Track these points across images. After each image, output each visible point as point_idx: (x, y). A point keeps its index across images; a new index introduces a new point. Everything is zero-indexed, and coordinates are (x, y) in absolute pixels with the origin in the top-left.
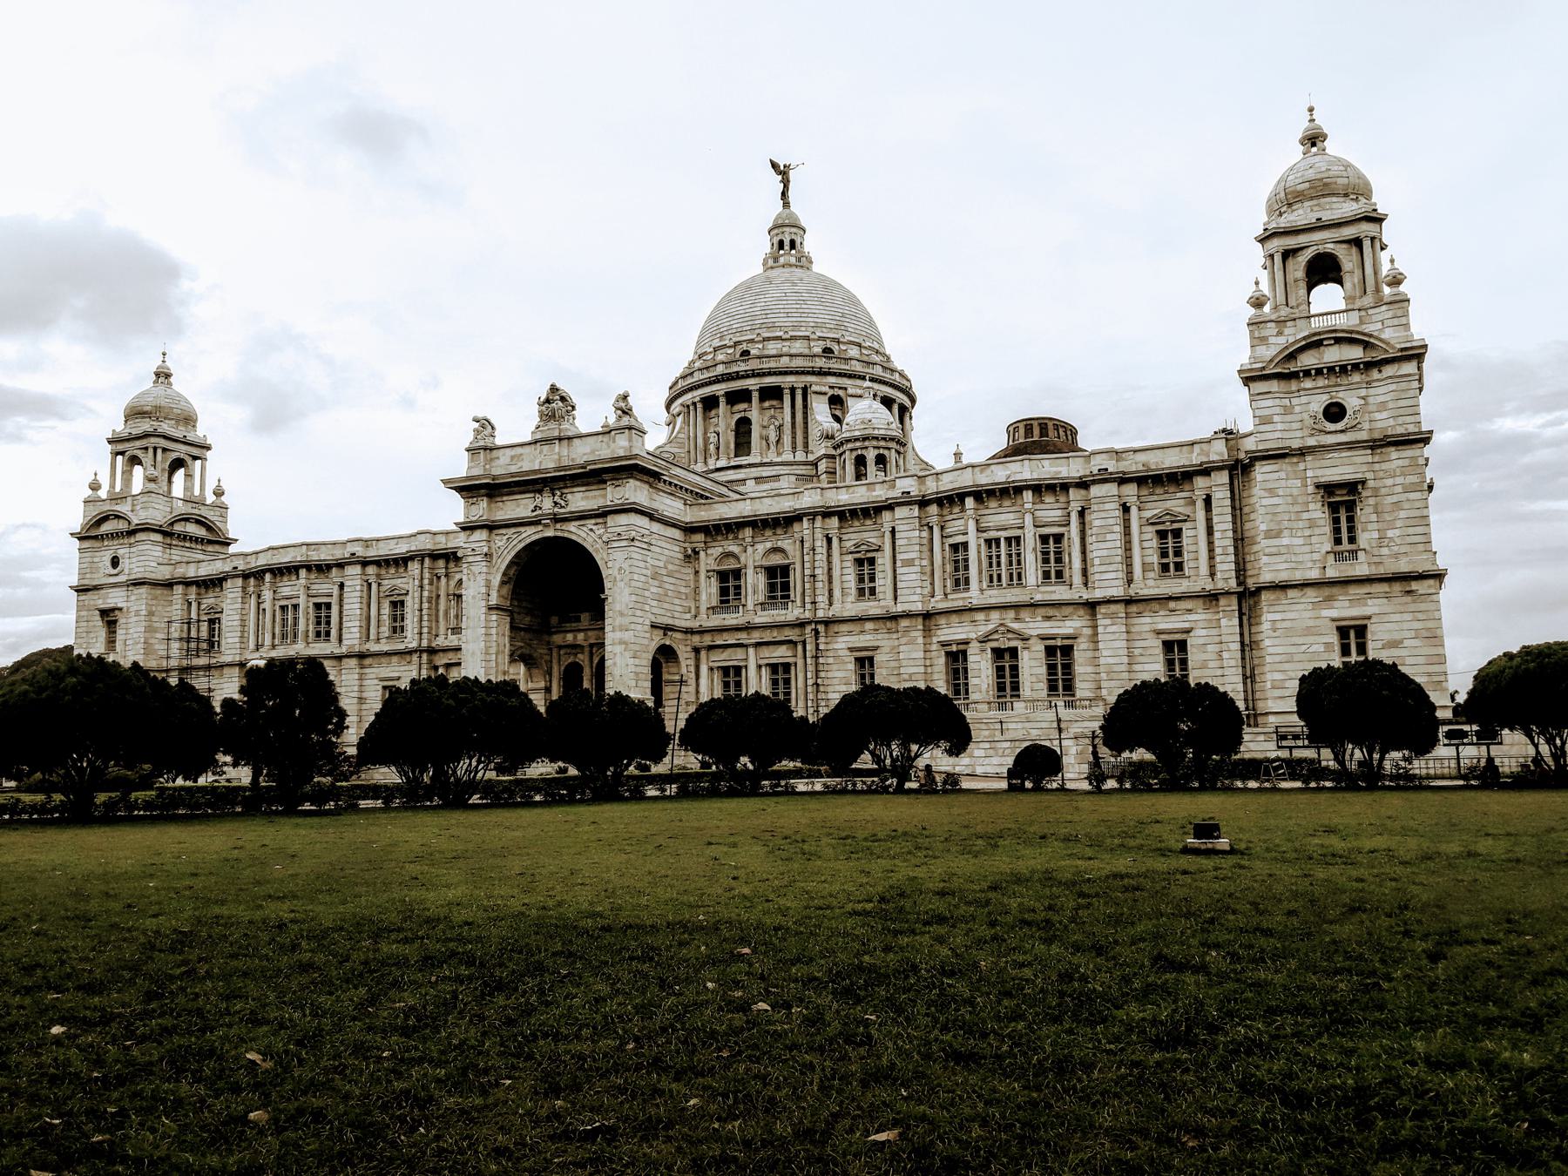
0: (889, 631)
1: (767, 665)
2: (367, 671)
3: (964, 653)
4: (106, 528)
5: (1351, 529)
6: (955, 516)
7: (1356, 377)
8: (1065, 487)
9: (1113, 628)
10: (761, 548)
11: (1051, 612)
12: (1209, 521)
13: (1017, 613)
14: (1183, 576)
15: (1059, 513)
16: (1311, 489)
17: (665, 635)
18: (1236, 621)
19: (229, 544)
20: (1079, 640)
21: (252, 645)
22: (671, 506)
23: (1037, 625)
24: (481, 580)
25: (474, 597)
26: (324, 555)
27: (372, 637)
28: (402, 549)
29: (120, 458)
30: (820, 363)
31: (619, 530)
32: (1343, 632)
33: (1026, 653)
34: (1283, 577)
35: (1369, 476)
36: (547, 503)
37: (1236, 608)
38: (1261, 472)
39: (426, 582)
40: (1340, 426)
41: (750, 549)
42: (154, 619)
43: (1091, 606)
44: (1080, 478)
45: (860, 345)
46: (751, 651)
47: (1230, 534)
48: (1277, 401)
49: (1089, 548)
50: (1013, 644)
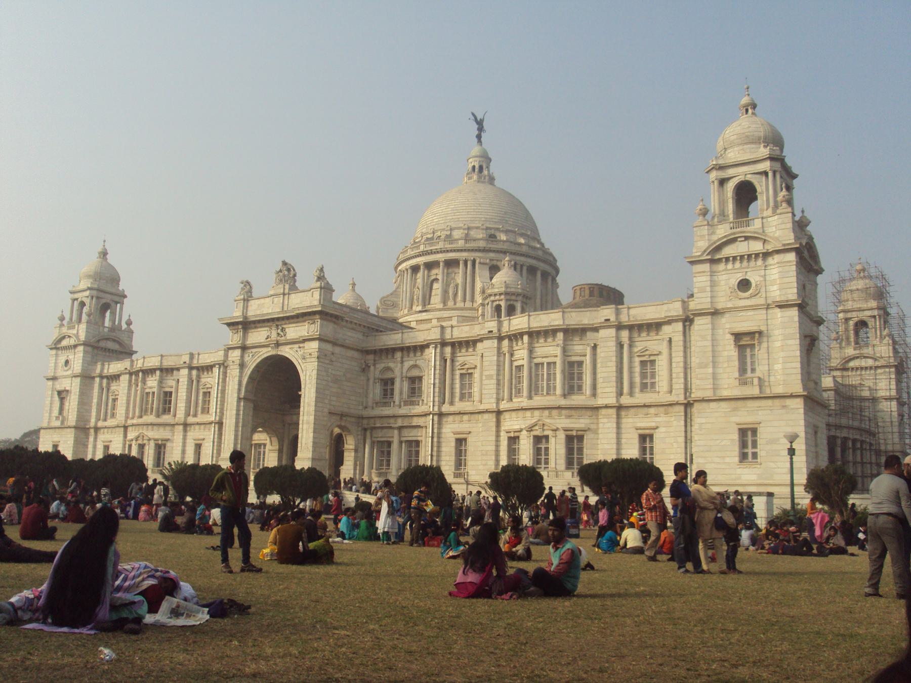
1: (407, 441)
2: (189, 434)
3: (518, 437)
4: (65, 343)
5: (752, 363)
7: (760, 262)
8: (582, 331)
9: (609, 425)
12: (670, 355)
13: (550, 413)
16: (729, 336)
17: (341, 419)
18: (683, 423)
19: (132, 354)
20: (587, 433)
22: (351, 336)
23: (562, 421)
26: (168, 363)
27: (191, 413)
30: (482, 244)
31: (310, 351)
32: (743, 432)
34: (709, 394)
35: (763, 328)
37: (683, 414)
38: (701, 325)
39: (221, 380)
40: (747, 294)
43: (597, 408)
44: (593, 324)
45: (514, 232)
46: (396, 432)
47: (682, 364)
49: (599, 370)
50: (546, 433)
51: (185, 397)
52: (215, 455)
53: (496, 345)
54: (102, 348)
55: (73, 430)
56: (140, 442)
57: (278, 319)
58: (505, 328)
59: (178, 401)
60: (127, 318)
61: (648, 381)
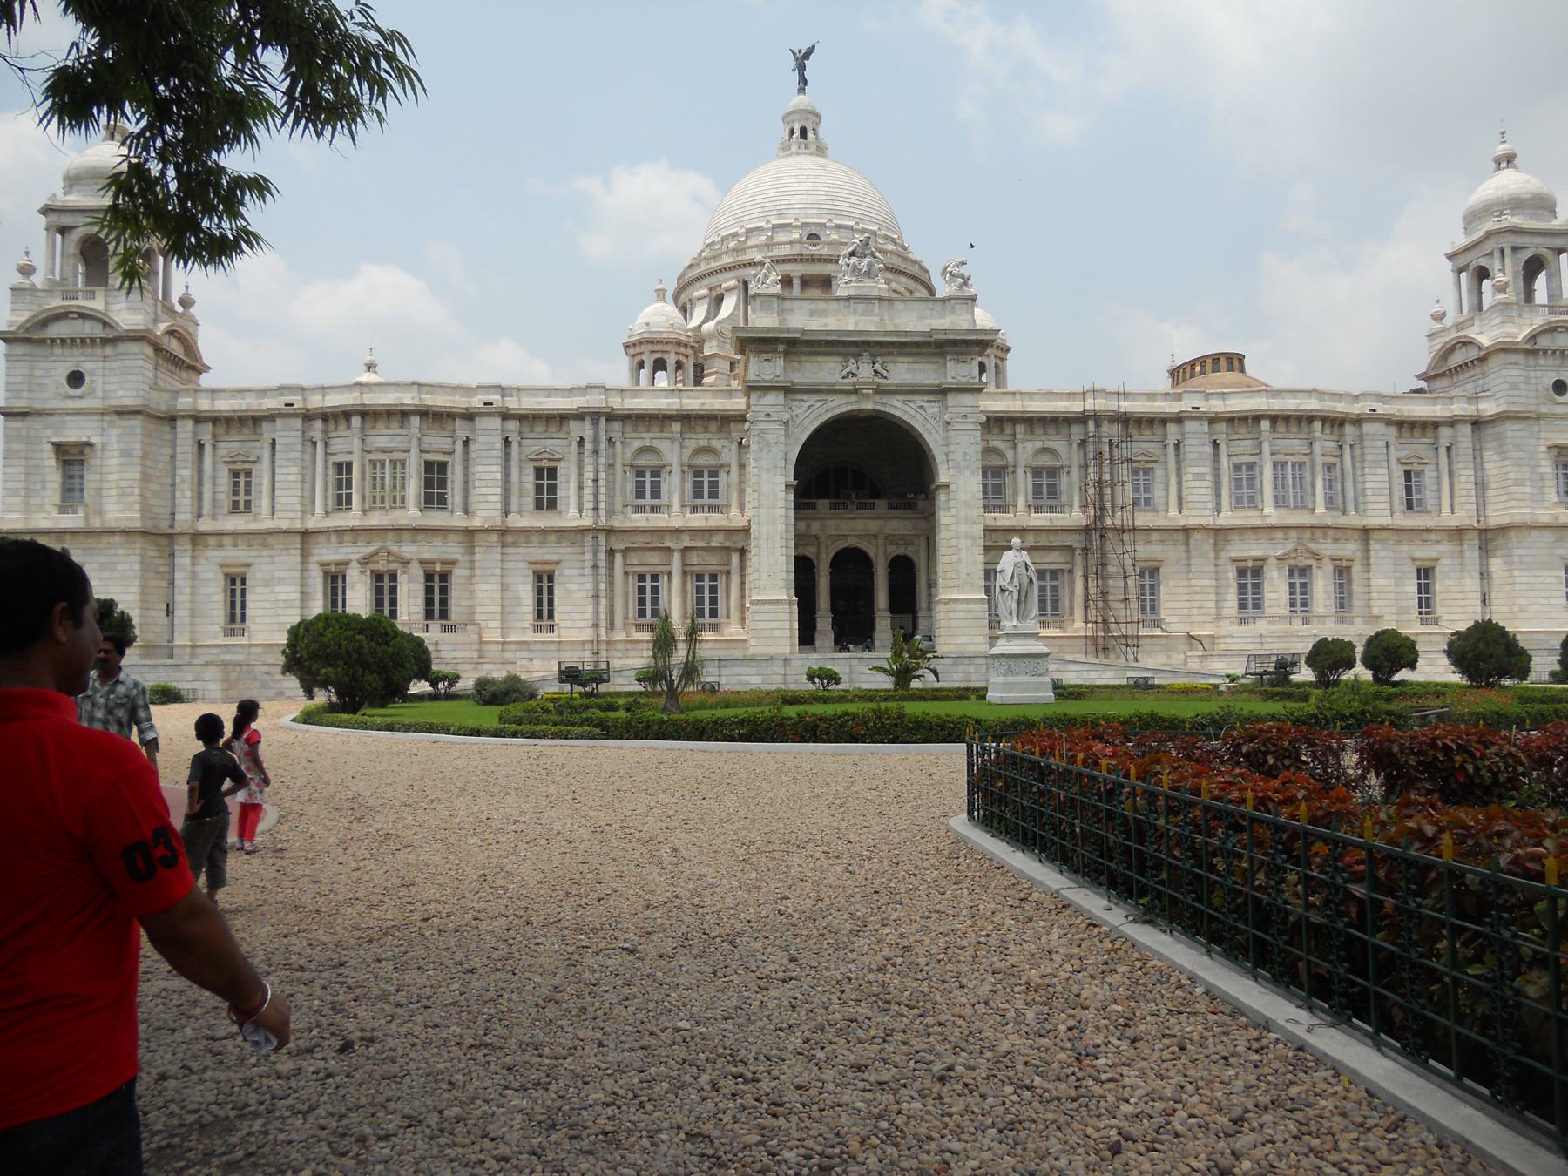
2: (510, 550)
13: (1313, 533)
15: (1332, 444)
19: (200, 372)
21: (319, 509)
23: (1328, 546)
24: (778, 451)
27: (514, 506)
29: (59, 237)
31: (964, 411)
33: (1320, 572)
36: (865, 371)
39: (603, 446)
41: (1020, 446)
42: (149, 463)
43: (1366, 532)
47: (1472, 479)
51: (499, 476)
52: (603, 593)
53: (1206, 429)
56: (381, 566)
58: (1217, 406)
60: (184, 290)
61: (1414, 497)
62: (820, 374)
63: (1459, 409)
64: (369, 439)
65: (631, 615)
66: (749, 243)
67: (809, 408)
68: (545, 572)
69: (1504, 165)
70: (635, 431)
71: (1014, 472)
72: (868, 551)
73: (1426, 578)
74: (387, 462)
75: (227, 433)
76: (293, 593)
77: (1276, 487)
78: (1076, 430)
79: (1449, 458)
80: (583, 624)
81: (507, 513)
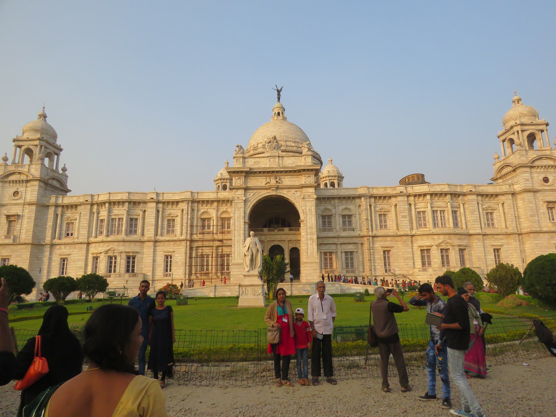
0: (397, 241)
1: (345, 252)
2: (158, 248)
6: (419, 202)
7: (552, 170)
9: (479, 244)
10: (341, 208)
11: (458, 236)
14: (495, 228)
15: (456, 204)
16: (541, 203)
20: (468, 247)
21: (93, 235)
24: (242, 209)
25: (238, 217)
27: (159, 233)
28: (177, 198)
29: (18, 149)
33: (453, 251)
34: (538, 229)
36: (273, 182)
39: (189, 212)
41: (337, 208)
43: (471, 235)
46: (339, 246)
48: (530, 175)
50: (448, 248)
51: (154, 223)
53: (406, 199)
54: (50, 185)
55: (30, 246)
56: (111, 254)
57: (277, 172)
59: (146, 225)
60: (64, 166)
61: (490, 222)
62: (258, 183)
63: (505, 188)
64: (112, 211)
65: (198, 270)
66: (258, 147)
67: (253, 195)
68: (169, 255)
69: (516, 103)
70: (202, 206)
71: (335, 217)
72: (282, 246)
73: (498, 252)
74: (117, 219)
75: (67, 210)
76: (82, 264)
77: (434, 219)
78: (357, 201)
79: (503, 207)
80: (180, 273)
81: (156, 234)
